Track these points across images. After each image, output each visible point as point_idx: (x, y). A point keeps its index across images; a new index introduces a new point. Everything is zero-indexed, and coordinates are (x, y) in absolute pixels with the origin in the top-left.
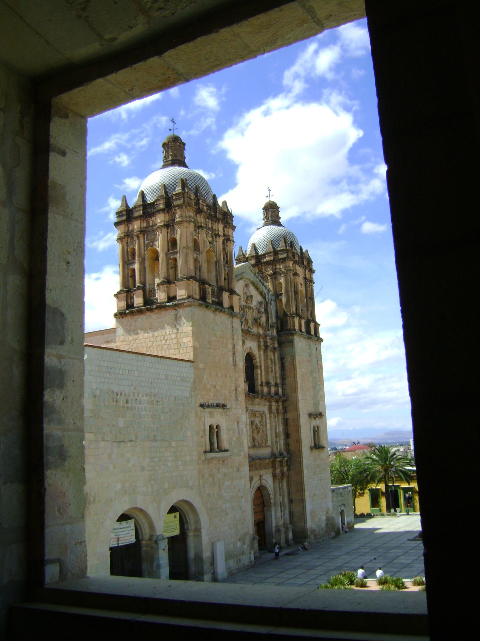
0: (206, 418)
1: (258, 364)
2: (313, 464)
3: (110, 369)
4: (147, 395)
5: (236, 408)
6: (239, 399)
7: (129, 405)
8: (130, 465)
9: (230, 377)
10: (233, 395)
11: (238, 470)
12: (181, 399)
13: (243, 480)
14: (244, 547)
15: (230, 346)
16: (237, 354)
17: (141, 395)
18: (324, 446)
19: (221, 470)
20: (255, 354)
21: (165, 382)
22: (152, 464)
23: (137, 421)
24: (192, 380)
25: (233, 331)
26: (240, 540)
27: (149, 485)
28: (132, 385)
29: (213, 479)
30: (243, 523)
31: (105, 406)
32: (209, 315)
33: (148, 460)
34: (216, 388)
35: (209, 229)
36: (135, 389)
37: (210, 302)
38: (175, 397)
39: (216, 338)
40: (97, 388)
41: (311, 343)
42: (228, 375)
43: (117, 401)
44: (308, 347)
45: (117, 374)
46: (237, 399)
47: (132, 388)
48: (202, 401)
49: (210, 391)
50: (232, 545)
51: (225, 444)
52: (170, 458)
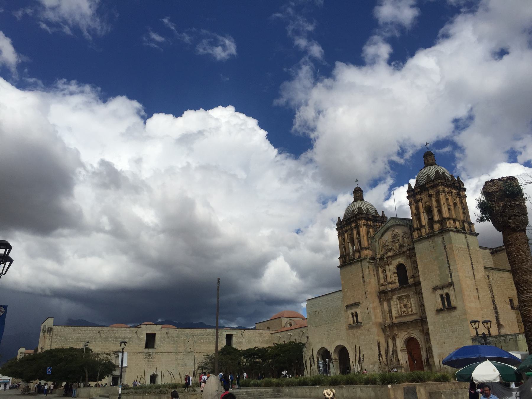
6: (368, 297)
7: (319, 314)
8: (321, 333)
10: (364, 296)
11: (369, 331)
13: (372, 336)
14: (375, 368)
15: (361, 275)
16: (365, 277)
19: (358, 332)
24: (342, 298)
25: (362, 267)
29: (354, 336)
30: (373, 356)
34: (354, 296)
35: (349, 229)
36: (321, 308)
37: (348, 261)
38: (335, 306)
39: (352, 275)
42: (360, 288)
44: (431, 242)
48: (347, 304)
51: (360, 320)
52: (334, 329)
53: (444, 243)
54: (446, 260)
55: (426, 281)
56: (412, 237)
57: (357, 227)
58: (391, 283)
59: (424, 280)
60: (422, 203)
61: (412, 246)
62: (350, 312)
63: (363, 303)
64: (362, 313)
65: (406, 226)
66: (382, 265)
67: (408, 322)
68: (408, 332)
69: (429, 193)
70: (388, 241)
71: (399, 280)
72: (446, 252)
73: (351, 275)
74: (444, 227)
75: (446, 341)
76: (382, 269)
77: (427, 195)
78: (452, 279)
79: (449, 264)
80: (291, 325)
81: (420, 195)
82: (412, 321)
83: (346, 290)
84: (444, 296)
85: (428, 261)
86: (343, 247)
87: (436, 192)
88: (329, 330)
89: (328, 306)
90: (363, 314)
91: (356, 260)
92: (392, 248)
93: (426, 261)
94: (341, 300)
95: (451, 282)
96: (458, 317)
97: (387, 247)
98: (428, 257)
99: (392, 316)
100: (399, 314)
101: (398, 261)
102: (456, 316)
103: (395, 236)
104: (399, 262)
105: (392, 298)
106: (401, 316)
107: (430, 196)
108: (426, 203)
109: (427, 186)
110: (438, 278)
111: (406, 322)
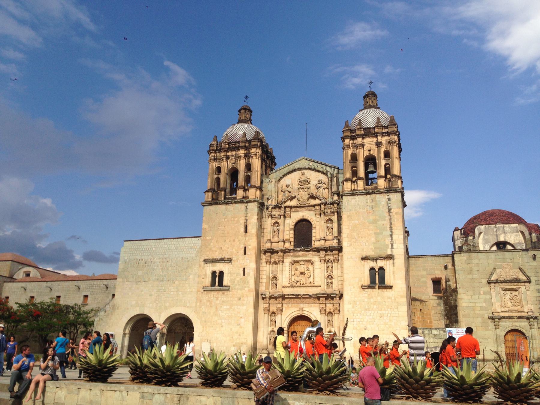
0: (208, 267)
1: (313, 226)
2: (366, 300)
3: (136, 249)
4: (160, 259)
5: (243, 259)
6: (249, 253)
7: (147, 264)
8: (143, 293)
9: (239, 241)
12: (187, 258)
13: (245, 307)
15: (242, 222)
17: (155, 259)
18: (391, 285)
19: (220, 299)
20: (309, 219)
21: (175, 250)
22: (159, 293)
23: (151, 272)
24: (198, 247)
26: (234, 346)
27: (155, 303)
28: (150, 255)
31: (131, 266)
32: (223, 207)
33: (155, 291)
35: (232, 156)
38: (182, 258)
39: (226, 219)
40: (127, 259)
41: (378, 196)
42: (237, 240)
43: (139, 263)
45: (141, 251)
46: (245, 254)
47: (150, 257)
48: (206, 258)
49: (216, 251)
50: (225, 348)
51: (225, 283)
52: (173, 290)
53: (389, 205)
54: (389, 226)
55: (352, 247)
56: (331, 188)
57: (248, 156)
58: (284, 241)
59: (350, 246)
60: (363, 149)
61: (330, 200)
62: (210, 268)
63: (238, 261)
64: (234, 274)
65: (325, 174)
66: (275, 215)
67: (304, 295)
68: (301, 309)
69: (377, 140)
70: (290, 186)
71: (295, 238)
72: (390, 216)
73: (225, 219)
74: (394, 186)
75: (368, 326)
76: (273, 221)
77: (374, 142)
78: (391, 251)
79: (391, 232)
80: (28, 275)
81: (363, 139)
82: (311, 295)
83: (210, 237)
84: (377, 270)
85: (359, 223)
86: (216, 178)
87: (387, 141)
88: (161, 291)
89: (167, 256)
90: (235, 275)
91: (239, 201)
92: (295, 197)
93: (357, 222)
94: (197, 250)
95: (391, 255)
96: (393, 298)
97: (287, 194)
98: (362, 218)
99: (276, 285)
100: (289, 283)
101: (302, 215)
102: (389, 298)
103: (304, 183)
104: (303, 216)
105: (283, 262)
106: (292, 286)
107: (378, 144)
108: (369, 151)
109: (376, 130)
110: (372, 247)
111: (300, 295)
